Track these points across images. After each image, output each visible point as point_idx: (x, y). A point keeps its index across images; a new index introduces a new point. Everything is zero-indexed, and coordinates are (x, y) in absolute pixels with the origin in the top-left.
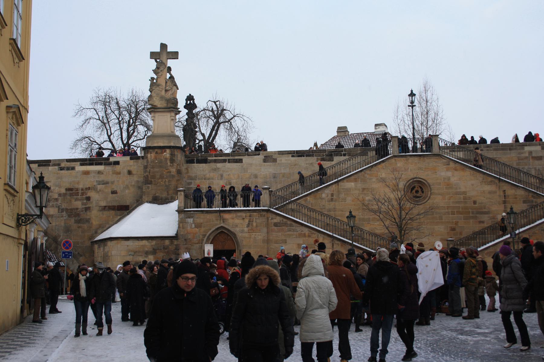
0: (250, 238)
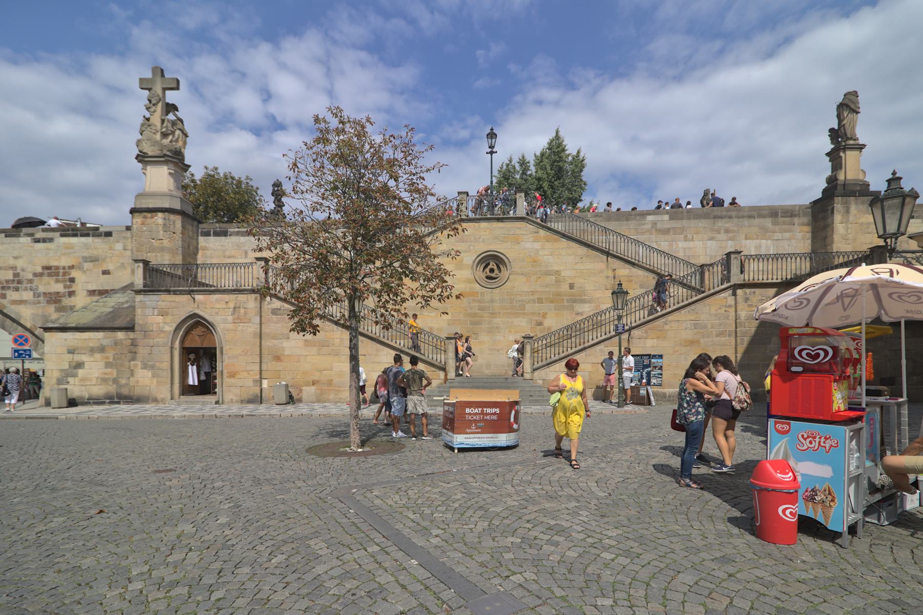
0: (236, 331)
